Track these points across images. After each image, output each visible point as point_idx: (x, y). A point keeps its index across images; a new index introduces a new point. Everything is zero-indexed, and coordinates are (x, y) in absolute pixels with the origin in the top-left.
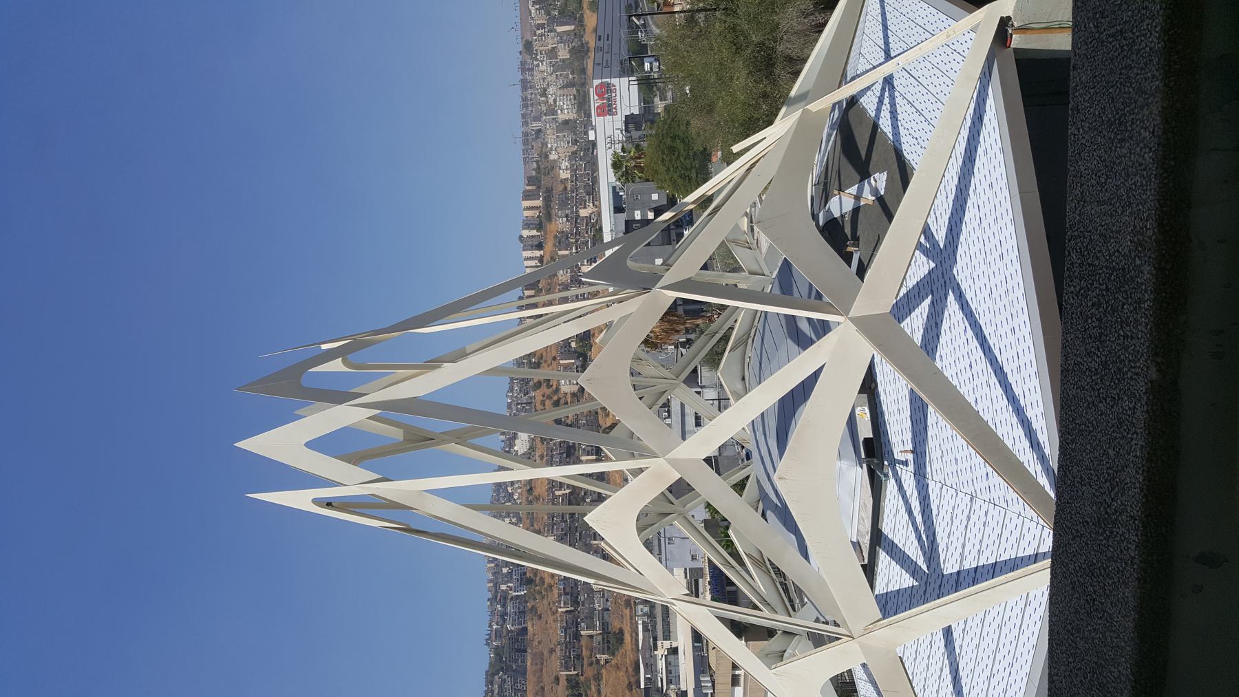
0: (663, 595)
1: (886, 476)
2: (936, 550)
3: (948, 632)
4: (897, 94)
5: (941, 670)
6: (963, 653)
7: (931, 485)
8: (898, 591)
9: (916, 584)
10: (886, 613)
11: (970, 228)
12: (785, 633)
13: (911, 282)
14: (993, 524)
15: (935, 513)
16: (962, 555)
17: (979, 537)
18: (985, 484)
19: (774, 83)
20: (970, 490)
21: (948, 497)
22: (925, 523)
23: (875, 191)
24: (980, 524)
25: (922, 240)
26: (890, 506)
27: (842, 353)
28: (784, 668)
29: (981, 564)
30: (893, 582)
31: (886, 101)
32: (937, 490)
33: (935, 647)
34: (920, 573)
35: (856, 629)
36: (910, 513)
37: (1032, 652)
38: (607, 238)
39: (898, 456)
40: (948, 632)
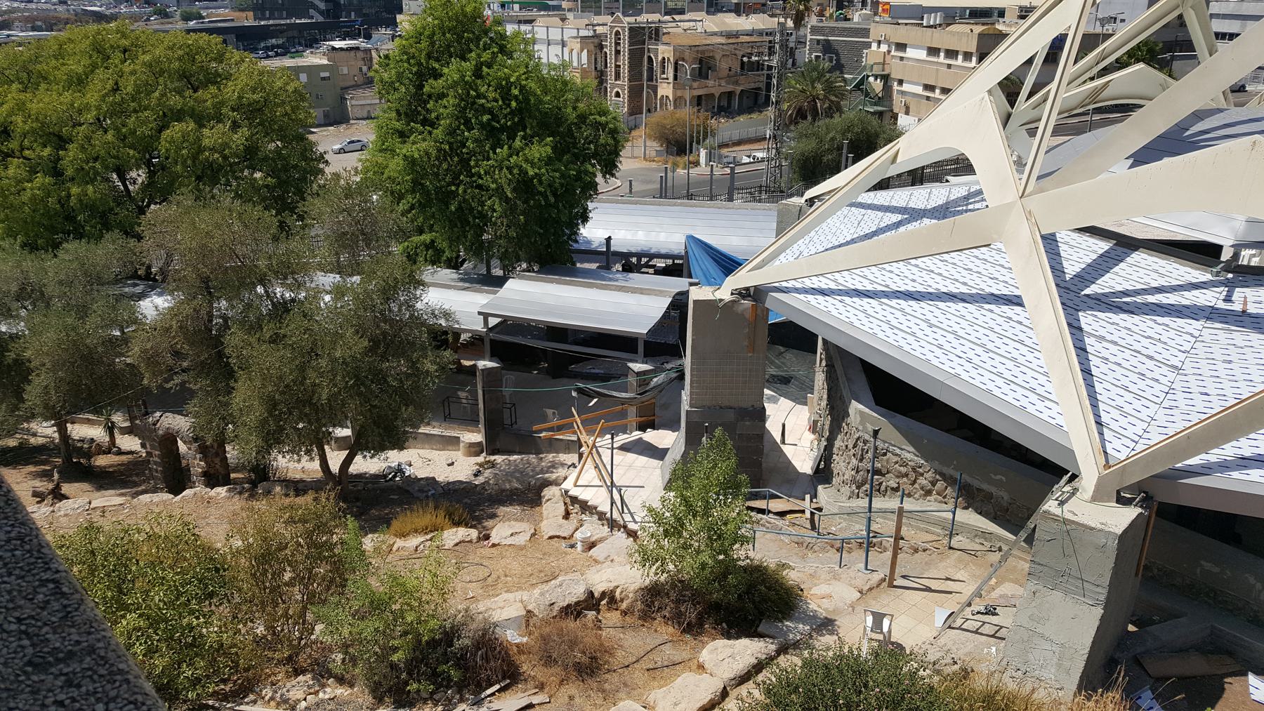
1: (1218, 274)
2: (1110, 310)
3: (1015, 301)
5: (965, 284)
6: (984, 312)
7: (1197, 324)
9: (1068, 277)
12: (1009, 115)
14: (1142, 384)
15: (1159, 319)
16: (1103, 338)
17: (1125, 364)
21: (1179, 340)
22: (1146, 304)
24: (1142, 369)
26: (1169, 268)
29: (1090, 357)
30: (1070, 251)
32: (1189, 329)
33: (991, 282)
34: (1080, 285)
35: (1034, 203)
36: (1160, 290)
37: (984, 387)
39: (1238, 293)
40: (1015, 301)
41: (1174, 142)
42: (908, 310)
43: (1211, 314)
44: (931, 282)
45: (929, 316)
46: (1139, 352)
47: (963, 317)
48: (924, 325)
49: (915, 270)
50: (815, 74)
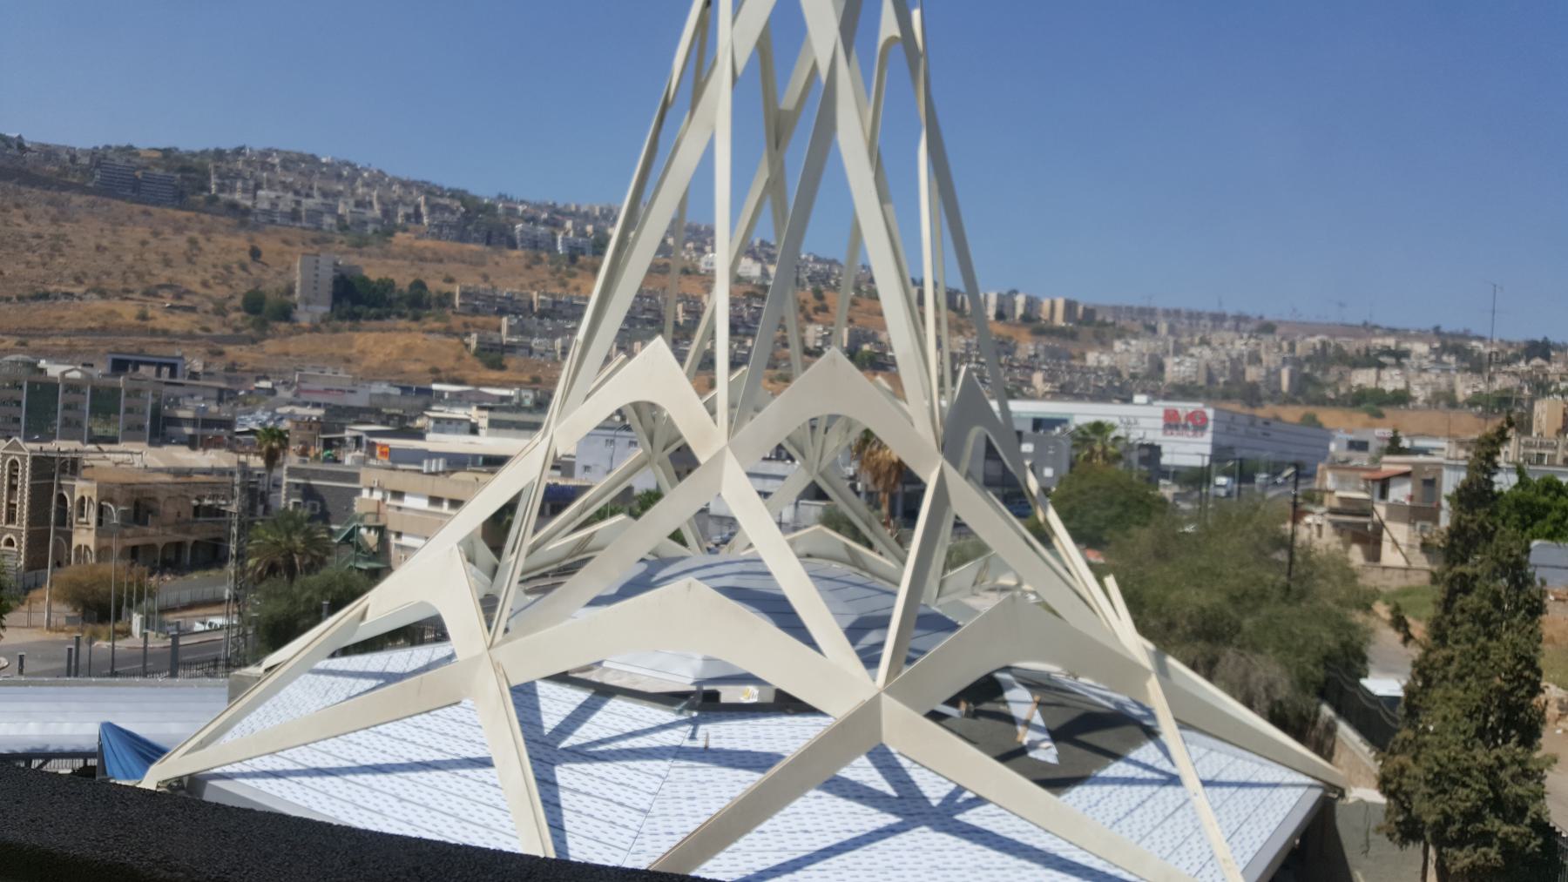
0: (558, 421)
1: (680, 712)
3: (486, 763)
4: (1155, 788)
5: (439, 750)
8: (538, 709)
9: (546, 731)
10: (515, 691)
11: (978, 855)
12: (495, 569)
13: (916, 774)
14: (612, 833)
16: (576, 791)
18: (661, 830)
19: (1185, 639)
20: (655, 810)
21: (648, 783)
23: (1034, 745)
25: (968, 795)
27: (836, 678)
28: (458, 560)
29: (565, 812)
31: (1148, 775)
32: (658, 771)
33: (467, 745)
35: (501, 653)
38: (1015, 406)
39: (703, 729)
40: (486, 763)
42: (377, 785)
43: (678, 753)
44: (403, 752)
45: (400, 790)
47: (435, 787)
48: (393, 801)
49: (386, 740)
50: (291, 523)
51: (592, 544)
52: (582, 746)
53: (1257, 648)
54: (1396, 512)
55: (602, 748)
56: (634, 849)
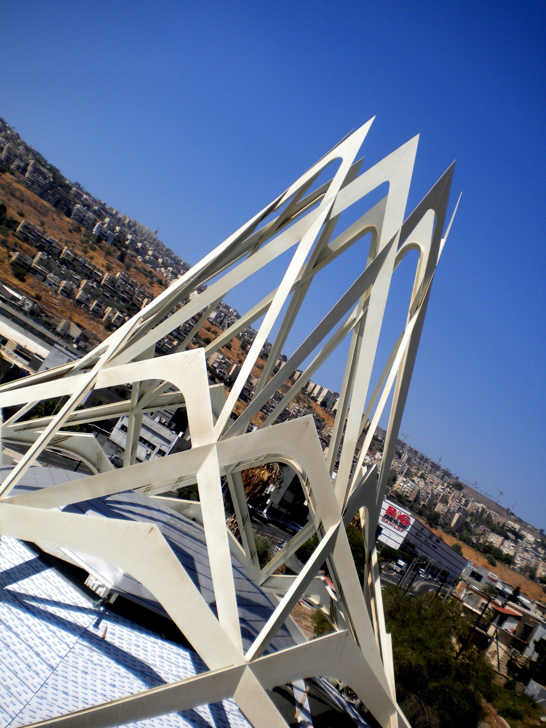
14: (27, 673)
20: (60, 668)
21: (59, 647)
22: (46, 612)
32: (67, 640)
39: (104, 623)
41: (103, 506)
46: (31, 648)
51: (64, 443)
52: (20, 594)
53: (430, 703)
54: (502, 636)
55: (34, 604)
56: (40, 694)
